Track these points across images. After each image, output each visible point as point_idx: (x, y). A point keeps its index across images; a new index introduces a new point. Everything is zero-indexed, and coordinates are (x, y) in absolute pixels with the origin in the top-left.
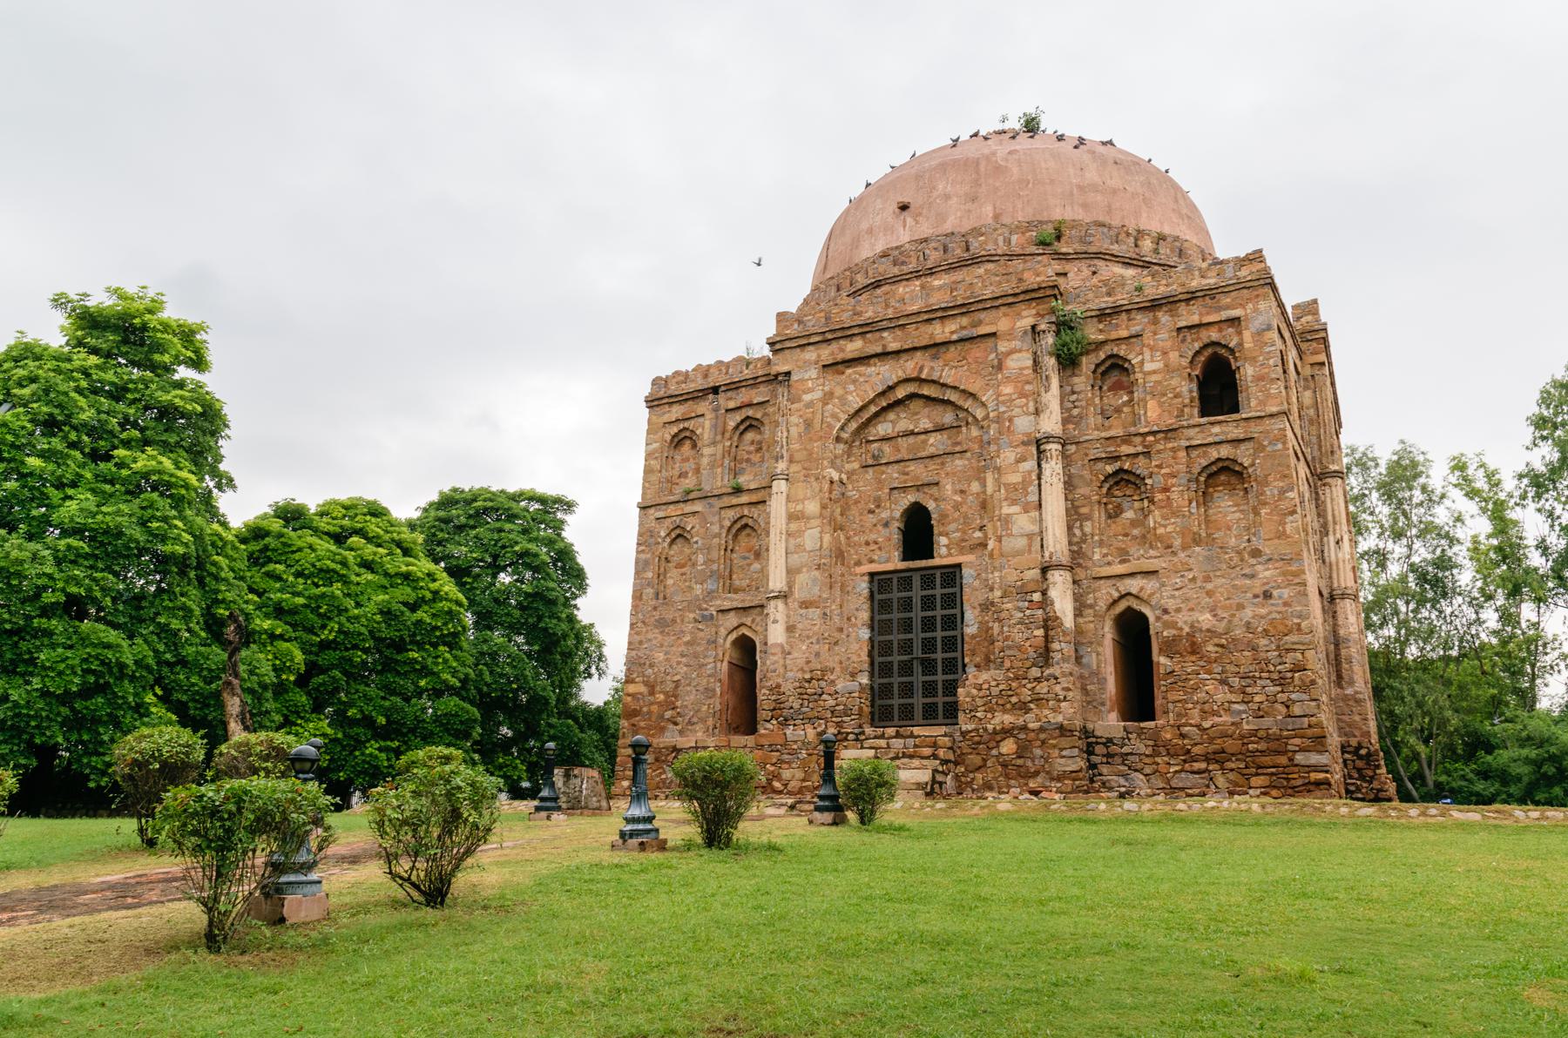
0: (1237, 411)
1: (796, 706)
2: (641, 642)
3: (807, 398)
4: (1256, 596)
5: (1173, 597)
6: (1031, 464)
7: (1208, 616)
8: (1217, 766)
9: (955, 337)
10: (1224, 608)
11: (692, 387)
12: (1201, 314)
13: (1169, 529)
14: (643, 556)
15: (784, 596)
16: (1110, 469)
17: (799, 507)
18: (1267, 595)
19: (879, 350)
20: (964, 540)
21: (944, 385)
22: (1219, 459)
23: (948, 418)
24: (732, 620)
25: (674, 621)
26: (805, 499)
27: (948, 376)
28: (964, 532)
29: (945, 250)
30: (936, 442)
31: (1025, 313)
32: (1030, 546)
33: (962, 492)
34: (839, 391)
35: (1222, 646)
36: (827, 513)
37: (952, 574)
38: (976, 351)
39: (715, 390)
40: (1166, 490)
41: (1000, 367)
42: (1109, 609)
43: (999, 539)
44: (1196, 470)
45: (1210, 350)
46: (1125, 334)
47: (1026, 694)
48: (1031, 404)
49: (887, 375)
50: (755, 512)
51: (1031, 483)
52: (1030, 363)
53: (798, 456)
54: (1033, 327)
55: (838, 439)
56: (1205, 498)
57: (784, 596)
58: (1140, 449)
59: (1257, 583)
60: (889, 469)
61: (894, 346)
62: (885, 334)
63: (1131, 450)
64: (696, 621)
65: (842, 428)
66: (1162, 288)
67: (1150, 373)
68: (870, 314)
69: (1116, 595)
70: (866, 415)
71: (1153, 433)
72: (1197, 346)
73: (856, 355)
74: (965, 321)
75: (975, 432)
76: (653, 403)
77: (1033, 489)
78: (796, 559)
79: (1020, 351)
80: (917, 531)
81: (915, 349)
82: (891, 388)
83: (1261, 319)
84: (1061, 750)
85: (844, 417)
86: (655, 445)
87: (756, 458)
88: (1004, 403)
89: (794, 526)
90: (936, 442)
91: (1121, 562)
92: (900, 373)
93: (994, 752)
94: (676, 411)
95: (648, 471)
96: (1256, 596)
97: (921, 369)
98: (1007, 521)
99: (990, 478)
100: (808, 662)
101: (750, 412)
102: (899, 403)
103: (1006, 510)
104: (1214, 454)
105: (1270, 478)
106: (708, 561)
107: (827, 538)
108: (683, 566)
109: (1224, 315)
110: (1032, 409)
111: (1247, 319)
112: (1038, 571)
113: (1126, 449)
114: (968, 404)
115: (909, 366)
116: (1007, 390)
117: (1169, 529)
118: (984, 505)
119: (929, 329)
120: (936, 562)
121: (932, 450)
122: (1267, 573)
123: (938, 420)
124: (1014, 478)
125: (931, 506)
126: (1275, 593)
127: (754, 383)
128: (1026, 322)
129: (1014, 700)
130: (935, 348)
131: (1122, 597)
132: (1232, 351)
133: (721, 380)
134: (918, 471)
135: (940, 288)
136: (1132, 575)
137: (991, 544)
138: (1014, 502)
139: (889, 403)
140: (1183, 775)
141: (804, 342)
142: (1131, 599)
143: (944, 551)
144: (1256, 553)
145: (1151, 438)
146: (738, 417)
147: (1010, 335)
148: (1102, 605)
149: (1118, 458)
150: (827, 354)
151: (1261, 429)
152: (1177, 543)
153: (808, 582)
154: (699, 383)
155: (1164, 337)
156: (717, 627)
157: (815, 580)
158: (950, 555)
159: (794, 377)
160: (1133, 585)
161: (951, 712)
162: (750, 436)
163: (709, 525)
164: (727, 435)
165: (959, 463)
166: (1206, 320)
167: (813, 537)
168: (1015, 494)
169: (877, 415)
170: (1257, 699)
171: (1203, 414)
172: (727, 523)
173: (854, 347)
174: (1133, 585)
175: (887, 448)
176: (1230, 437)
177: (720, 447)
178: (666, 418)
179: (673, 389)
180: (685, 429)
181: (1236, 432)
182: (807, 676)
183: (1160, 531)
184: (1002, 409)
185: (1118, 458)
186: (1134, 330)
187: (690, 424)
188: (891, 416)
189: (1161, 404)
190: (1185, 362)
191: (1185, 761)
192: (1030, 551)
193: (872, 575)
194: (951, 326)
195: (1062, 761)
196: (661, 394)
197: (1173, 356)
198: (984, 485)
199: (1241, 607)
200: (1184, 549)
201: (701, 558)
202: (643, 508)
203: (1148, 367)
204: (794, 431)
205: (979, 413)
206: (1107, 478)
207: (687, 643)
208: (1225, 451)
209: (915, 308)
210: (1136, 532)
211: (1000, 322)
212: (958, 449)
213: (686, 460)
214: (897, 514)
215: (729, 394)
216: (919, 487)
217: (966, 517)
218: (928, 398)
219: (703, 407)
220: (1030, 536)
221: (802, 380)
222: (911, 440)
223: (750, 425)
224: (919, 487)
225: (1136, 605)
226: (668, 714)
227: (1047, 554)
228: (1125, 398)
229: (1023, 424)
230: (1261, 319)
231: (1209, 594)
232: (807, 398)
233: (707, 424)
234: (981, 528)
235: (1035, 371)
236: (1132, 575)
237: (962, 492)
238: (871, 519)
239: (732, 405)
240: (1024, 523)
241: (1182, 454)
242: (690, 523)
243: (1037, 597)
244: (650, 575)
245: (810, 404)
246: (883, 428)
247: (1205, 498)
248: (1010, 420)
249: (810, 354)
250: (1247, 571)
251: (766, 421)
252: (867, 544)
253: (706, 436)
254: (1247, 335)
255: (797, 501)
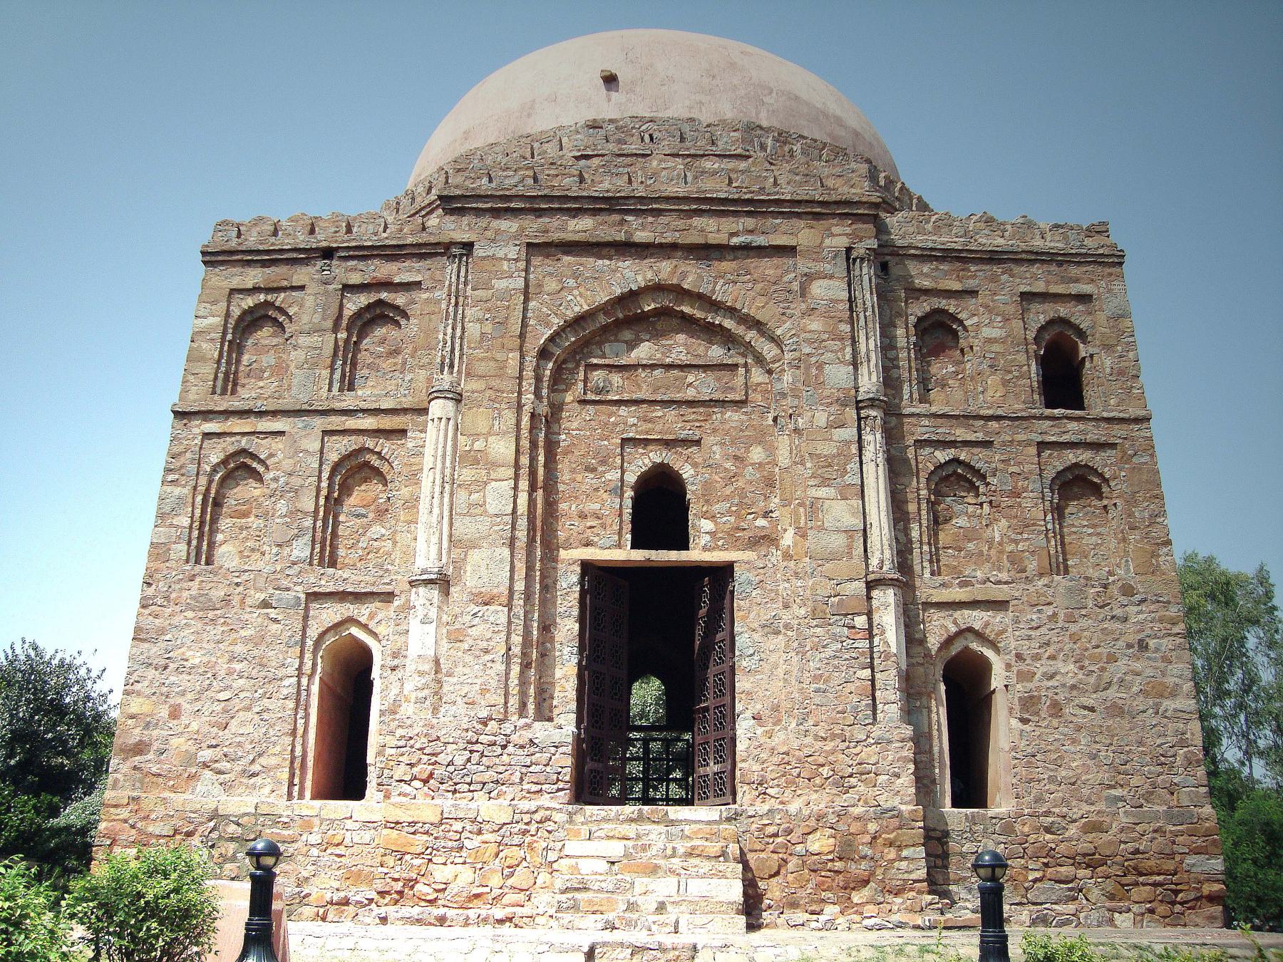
0: (1082, 408)
1: (459, 761)
2: (162, 631)
3: (500, 284)
4: (1129, 646)
5: (1029, 638)
6: (850, 433)
7: (1072, 666)
8: (1088, 872)
9: (735, 241)
10: (1095, 659)
11: (288, 243)
12: (1048, 283)
13: (1020, 547)
14: (177, 491)
15: (442, 583)
16: (942, 456)
17: (478, 446)
18: (1143, 646)
19: (621, 237)
20: (738, 528)
21: (715, 306)
22: (1076, 465)
23: (716, 353)
24: (329, 614)
25: (226, 601)
26: (489, 434)
27: (723, 293)
28: (739, 517)
29: (682, 139)
30: (700, 386)
31: (835, 230)
32: (850, 547)
33: (736, 458)
34: (551, 285)
35: (1092, 709)
36: (525, 460)
37: (722, 574)
38: (768, 267)
39: (328, 253)
40: (1015, 494)
41: (804, 292)
42: (940, 649)
43: (802, 533)
44: (1050, 474)
45: (1056, 329)
46: (957, 286)
47: (844, 764)
48: (849, 350)
49: (629, 274)
50: (385, 446)
51: (848, 459)
52: (845, 295)
53: (481, 368)
54: (849, 250)
55: (544, 354)
56: (1059, 512)
57: (442, 583)
58: (980, 436)
59: (1129, 627)
60: (623, 411)
61: (641, 236)
62: (630, 218)
63: (972, 437)
64: (265, 604)
65: (551, 339)
66: (1001, 241)
67: (989, 341)
68: (606, 185)
69: (953, 629)
70: (591, 327)
71: (998, 418)
72: (1042, 319)
73: (577, 237)
74: (750, 222)
75: (758, 376)
76: (213, 258)
77: (853, 466)
78: (465, 527)
79: (831, 277)
80: (660, 507)
81: (674, 247)
82: (631, 297)
83: (1116, 302)
84: (900, 848)
85: (557, 322)
86: (211, 320)
87: (386, 365)
88: (809, 342)
89: (466, 474)
90: (700, 386)
91: (963, 584)
92: (649, 275)
93: (799, 848)
94: (254, 276)
95: (194, 357)
96: (1129, 646)
97: (684, 275)
98: (814, 508)
99: (784, 448)
100: (484, 691)
101: (384, 295)
102: (643, 318)
103: (814, 493)
104: (1071, 457)
105: (1140, 496)
106: (294, 513)
107: (523, 499)
108: (245, 515)
109: (1074, 289)
110: (848, 357)
111: (1099, 299)
112: (860, 587)
113: (961, 434)
114: (751, 335)
115: (664, 270)
116: (815, 325)
117: (1020, 547)
118: (770, 483)
119: (697, 221)
120: (696, 554)
121: (690, 394)
122: (1141, 617)
123: (701, 351)
124: (827, 449)
125: (687, 472)
126: (1152, 643)
127: (394, 253)
128: (843, 242)
129: (825, 771)
130: (705, 252)
131: (960, 633)
132: (1082, 334)
133: (342, 240)
134: (672, 422)
135: (714, 173)
136: (973, 604)
137: (788, 539)
138: (825, 482)
139: (628, 317)
140: (1047, 884)
141: (501, 206)
142: (969, 635)
143: (705, 539)
144: (1128, 591)
145: (994, 425)
146: (363, 300)
147: (816, 253)
148: (933, 642)
149: (952, 444)
150: (533, 227)
151: (1123, 433)
152: (1032, 566)
153: (490, 567)
154: (302, 240)
155: (1005, 299)
156: (306, 618)
157: (501, 561)
158: (716, 548)
159: (478, 252)
160: (976, 618)
161: (724, 788)
162: (380, 332)
163: (298, 455)
164: (344, 323)
165: (733, 416)
166: (1054, 289)
167: (501, 496)
168: (827, 471)
169: (605, 329)
170: (1135, 781)
171: (1047, 407)
172: (334, 457)
173: (580, 228)
174: (976, 618)
175: (616, 379)
176: (1090, 438)
177: (330, 338)
178: (236, 282)
179: (252, 240)
180: (267, 304)
181: (1094, 433)
182: (484, 714)
183: (1009, 548)
184: (807, 350)
185: (952, 444)
186: (971, 284)
187: (280, 299)
188: (627, 335)
189: (1005, 383)
190: (1031, 335)
191: (1046, 865)
192: (850, 553)
193: (587, 567)
194: (729, 224)
195: (904, 864)
196: (233, 244)
197: (1017, 324)
198: (771, 450)
199: (1112, 659)
200: (1041, 575)
201: (282, 507)
202: (179, 415)
203: (987, 332)
204: (473, 329)
205: (769, 350)
206: (940, 466)
207: (246, 640)
208: (1084, 456)
209: (679, 190)
210: (971, 546)
211: (803, 234)
212: (730, 397)
213: (261, 349)
214: (631, 478)
215: (352, 263)
216: (668, 444)
217: (742, 493)
218: (683, 316)
219: (301, 275)
220: (849, 532)
221: (493, 257)
222: (657, 372)
223: (378, 315)
224: (668, 444)
225: (975, 646)
226: (206, 755)
227: (874, 562)
228: (951, 369)
229: (838, 375)
230: (1116, 302)
231: (1075, 638)
232: (500, 284)
233: (310, 301)
234: (766, 514)
235: (851, 309)
236: (973, 604)
237: (736, 458)
238: (590, 480)
239: (355, 279)
240: (841, 513)
241: (1033, 450)
242: (262, 447)
243: (861, 621)
244: (185, 521)
245: (507, 295)
246: (613, 353)
247: (1059, 512)
248: (820, 366)
249: (508, 225)
250: (1118, 612)
251: (413, 310)
252: (583, 516)
253: (305, 319)
254: (1101, 317)
255: (476, 436)
